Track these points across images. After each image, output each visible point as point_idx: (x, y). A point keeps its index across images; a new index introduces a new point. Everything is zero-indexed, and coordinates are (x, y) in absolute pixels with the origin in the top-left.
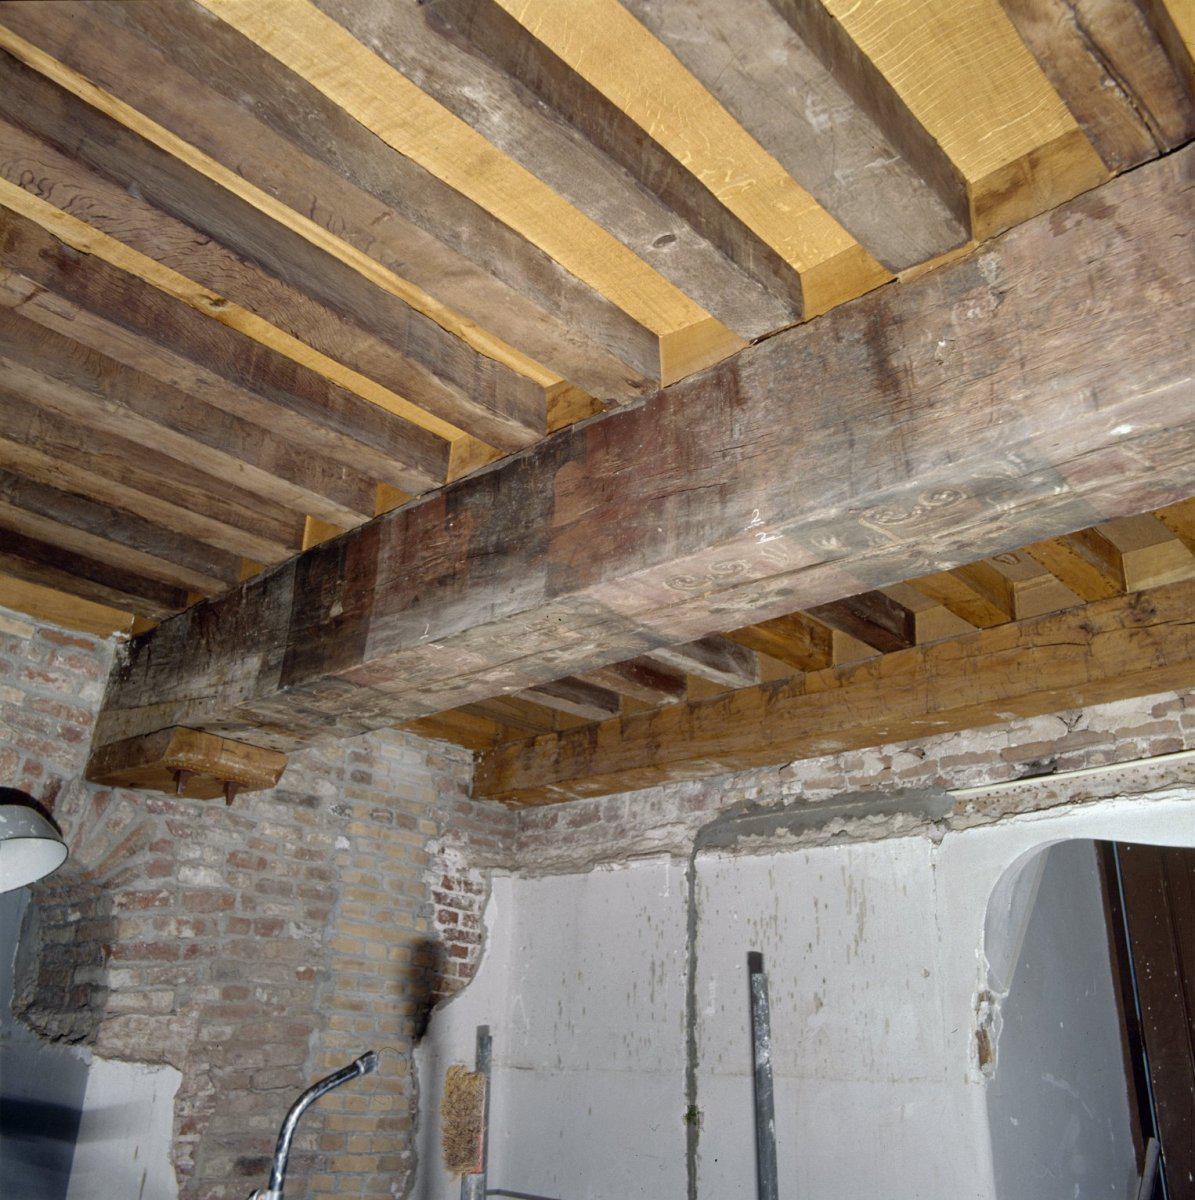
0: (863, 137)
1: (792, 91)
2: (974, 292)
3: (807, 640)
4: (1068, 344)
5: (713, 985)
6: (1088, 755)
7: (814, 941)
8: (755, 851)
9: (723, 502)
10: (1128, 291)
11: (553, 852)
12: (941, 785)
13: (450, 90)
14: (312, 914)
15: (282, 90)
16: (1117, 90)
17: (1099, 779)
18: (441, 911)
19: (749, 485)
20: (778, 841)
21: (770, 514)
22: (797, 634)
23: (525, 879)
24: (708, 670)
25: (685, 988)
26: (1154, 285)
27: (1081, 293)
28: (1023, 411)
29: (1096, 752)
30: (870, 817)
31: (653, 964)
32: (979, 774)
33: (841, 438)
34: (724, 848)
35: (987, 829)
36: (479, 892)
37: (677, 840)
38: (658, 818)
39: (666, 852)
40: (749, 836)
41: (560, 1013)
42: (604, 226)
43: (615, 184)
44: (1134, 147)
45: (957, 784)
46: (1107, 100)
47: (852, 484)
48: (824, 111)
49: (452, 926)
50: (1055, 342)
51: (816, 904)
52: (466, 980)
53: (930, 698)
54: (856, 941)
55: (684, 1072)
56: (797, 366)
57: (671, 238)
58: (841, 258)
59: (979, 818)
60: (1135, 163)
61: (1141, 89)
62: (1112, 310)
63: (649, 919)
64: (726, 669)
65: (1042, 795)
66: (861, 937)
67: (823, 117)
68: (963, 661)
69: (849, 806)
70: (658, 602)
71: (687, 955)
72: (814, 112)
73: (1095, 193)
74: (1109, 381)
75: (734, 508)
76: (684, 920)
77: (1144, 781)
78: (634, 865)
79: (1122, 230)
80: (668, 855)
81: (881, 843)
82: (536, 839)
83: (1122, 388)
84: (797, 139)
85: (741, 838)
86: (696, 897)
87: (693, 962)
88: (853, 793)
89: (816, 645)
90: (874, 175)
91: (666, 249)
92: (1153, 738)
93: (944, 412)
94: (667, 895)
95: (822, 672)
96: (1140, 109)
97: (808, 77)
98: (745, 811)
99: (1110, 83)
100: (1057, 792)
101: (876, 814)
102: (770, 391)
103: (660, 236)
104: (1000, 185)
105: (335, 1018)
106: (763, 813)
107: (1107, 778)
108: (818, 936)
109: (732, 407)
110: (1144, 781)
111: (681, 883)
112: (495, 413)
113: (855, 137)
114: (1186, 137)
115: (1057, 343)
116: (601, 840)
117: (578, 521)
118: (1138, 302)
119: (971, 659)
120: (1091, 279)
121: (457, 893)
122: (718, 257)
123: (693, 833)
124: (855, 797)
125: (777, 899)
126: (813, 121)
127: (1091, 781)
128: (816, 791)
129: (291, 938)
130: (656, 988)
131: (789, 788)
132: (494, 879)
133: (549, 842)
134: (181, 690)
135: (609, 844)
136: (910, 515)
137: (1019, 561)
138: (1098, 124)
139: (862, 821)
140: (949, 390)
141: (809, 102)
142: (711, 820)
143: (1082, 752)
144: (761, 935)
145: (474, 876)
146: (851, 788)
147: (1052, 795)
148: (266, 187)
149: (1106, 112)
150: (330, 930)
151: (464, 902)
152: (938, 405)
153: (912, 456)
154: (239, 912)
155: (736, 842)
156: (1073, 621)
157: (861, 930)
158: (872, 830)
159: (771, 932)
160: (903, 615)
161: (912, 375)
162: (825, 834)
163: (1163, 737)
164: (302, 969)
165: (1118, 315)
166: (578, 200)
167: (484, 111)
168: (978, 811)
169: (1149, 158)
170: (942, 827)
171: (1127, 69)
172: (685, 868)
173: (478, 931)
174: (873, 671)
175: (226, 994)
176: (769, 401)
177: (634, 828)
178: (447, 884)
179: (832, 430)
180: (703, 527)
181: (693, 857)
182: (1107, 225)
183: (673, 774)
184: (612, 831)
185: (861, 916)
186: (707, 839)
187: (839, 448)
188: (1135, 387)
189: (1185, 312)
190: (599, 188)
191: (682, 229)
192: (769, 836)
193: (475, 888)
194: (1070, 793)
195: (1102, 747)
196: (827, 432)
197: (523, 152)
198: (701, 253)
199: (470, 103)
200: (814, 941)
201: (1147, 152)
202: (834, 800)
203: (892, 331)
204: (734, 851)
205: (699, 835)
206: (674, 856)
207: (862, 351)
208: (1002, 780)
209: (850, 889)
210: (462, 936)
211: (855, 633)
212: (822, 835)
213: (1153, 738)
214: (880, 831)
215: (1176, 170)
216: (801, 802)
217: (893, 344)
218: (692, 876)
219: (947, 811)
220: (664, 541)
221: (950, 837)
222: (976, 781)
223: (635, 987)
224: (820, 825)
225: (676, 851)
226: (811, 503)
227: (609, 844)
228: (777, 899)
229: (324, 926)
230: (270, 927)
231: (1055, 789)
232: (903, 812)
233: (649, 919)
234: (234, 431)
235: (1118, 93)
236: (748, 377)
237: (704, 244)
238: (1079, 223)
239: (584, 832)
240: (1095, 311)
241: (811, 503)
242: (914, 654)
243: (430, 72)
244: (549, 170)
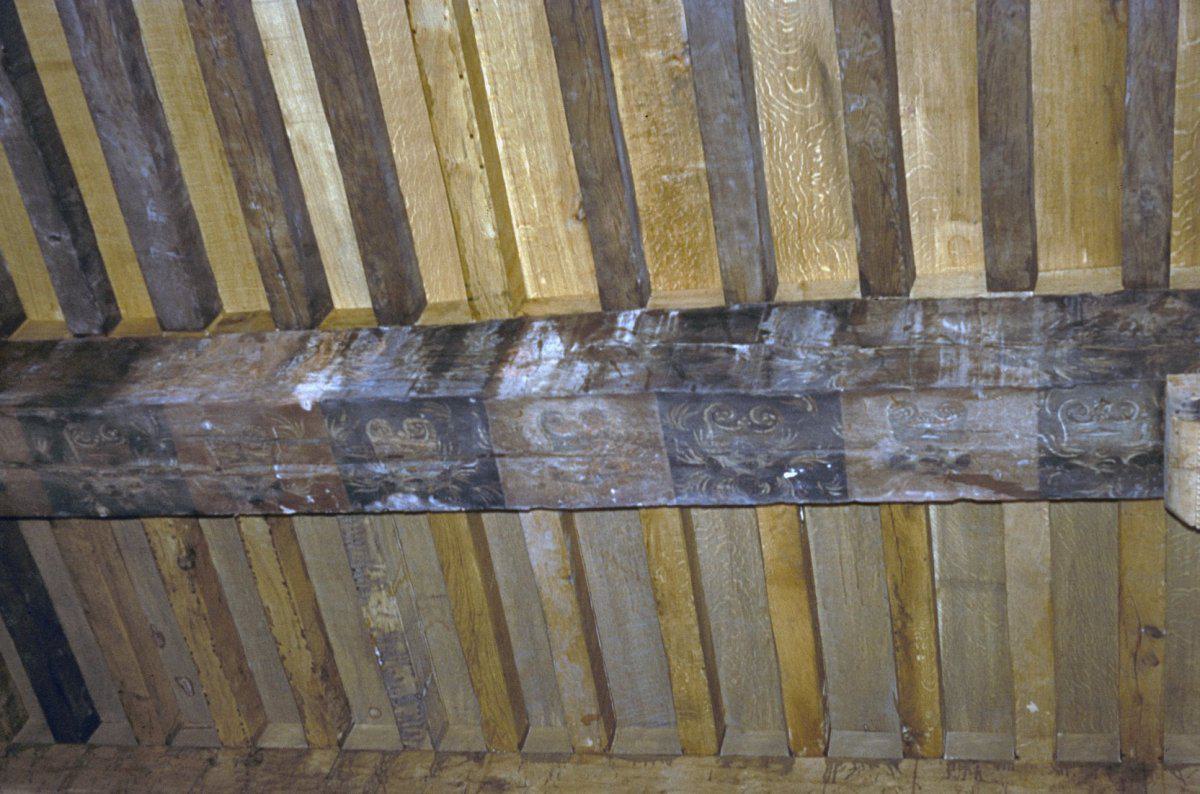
1: (145, 192)
57: (58, 239)
58: (146, 320)
67: (154, 214)
79: (262, 349)
91: (53, 244)
97: (154, 190)
99: (280, 276)
104: (235, 318)
122: (77, 264)
156: (206, 755)
160: (90, 712)
166: (23, 188)
182: (259, 345)
191: (67, 237)
237: (74, 252)
242: (80, 749)
244: (18, 163)
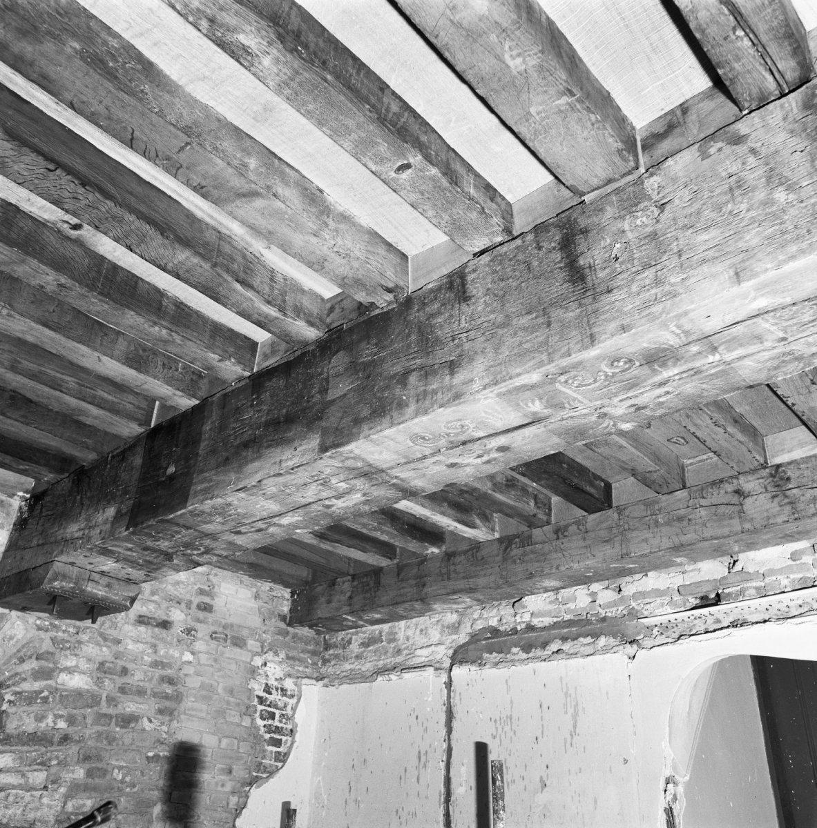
0: (551, 78)
1: (493, 37)
2: (641, 206)
3: (532, 503)
4: (714, 238)
6: (742, 592)
8: (496, 664)
9: (452, 374)
10: (760, 195)
11: (347, 666)
12: (633, 614)
13: (229, 37)
14: (160, 711)
15: (105, 43)
16: (746, 39)
17: (753, 609)
18: (262, 711)
19: (471, 360)
20: (513, 657)
21: (487, 381)
22: (524, 499)
23: (327, 687)
24: (460, 526)
25: (443, 772)
26: (780, 189)
27: (725, 198)
28: (681, 291)
29: (750, 587)
30: (581, 639)
31: (419, 752)
32: (663, 605)
33: (540, 320)
34: (473, 662)
35: (670, 647)
36: (292, 696)
37: (438, 657)
38: (425, 640)
40: (491, 653)
42: (355, 156)
43: (362, 119)
44: (760, 89)
45: (646, 613)
46: (739, 49)
47: (549, 354)
48: (519, 55)
49: (270, 722)
50: (704, 236)
51: (541, 706)
52: (280, 765)
53: (624, 546)
54: (571, 735)
56: (508, 270)
57: (408, 166)
58: (542, 190)
60: (763, 102)
61: (764, 38)
62: (748, 210)
64: (473, 526)
65: (710, 620)
66: (575, 732)
67: (519, 60)
68: (648, 519)
70: (406, 457)
71: (445, 746)
72: (511, 56)
73: (731, 126)
74: (748, 263)
75: (459, 378)
76: (443, 718)
77: (787, 610)
78: (407, 676)
79: (753, 151)
80: (432, 669)
82: (336, 656)
83: (758, 267)
84: (499, 80)
85: (486, 655)
87: (449, 751)
88: (568, 621)
89: (539, 508)
90: (560, 111)
92: (792, 576)
93: (616, 296)
94: (430, 699)
95: (545, 528)
96: (764, 54)
97: (505, 25)
98: (489, 635)
99: (740, 33)
100: (721, 618)
102: (488, 289)
103: (400, 164)
104: (660, 129)
106: (501, 637)
107: (759, 608)
108: (543, 733)
109: (460, 304)
110: (787, 610)
112: (285, 314)
113: (544, 78)
114: (800, 81)
115: (707, 237)
116: (383, 657)
117: (345, 395)
118: (768, 202)
119: (654, 517)
120: (731, 189)
121: (275, 697)
122: (445, 182)
123: (451, 652)
124: (570, 623)
125: (512, 702)
126: (511, 63)
128: (541, 619)
129: (144, 730)
131: (521, 617)
133: (346, 659)
134: (60, 534)
135: (388, 661)
136: (595, 381)
137: (687, 443)
138: (732, 69)
139: (576, 642)
140: (623, 280)
141: (507, 47)
142: (464, 641)
143: (738, 588)
144: (500, 728)
145: (289, 684)
146: (567, 617)
147: (718, 621)
148: (92, 118)
149: (738, 59)
150: (175, 724)
151: (280, 704)
152: (615, 291)
153: (595, 330)
154: (104, 708)
155: (481, 658)
156: (729, 488)
157: (575, 727)
158: (582, 649)
159: (507, 728)
160: (603, 484)
161: (595, 270)
162: (548, 652)
163: (800, 576)
164: (151, 754)
165: (753, 213)
166: (335, 135)
167: (257, 55)
168: (662, 634)
169: (773, 98)
170: (635, 646)
171: (754, 20)
172: (444, 678)
173: (290, 727)
174: (581, 527)
175: (89, 774)
176: (487, 297)
177: (407, 648)
178: (268, 690)
179: (534, 315)
180: (436, 393)
182: (742, 149)
183: (435, 606)
184: (391, 650)
185: (575, 716)
186: (460, 656)
187: (539, 328)
188: (769, 266)
189: (806, 206)
190: (350, 123)
191: (416, 159)
193: (289, 693)
195: (754, 584)
196: (531, 317)
197: (289, 91)
198: (433, 179)
199: (245, 49)
200: (539, 734)
201: (770, 94)
202: (555, 626)
203: (580, 239)
204: (480, 665)
205: (455, 653)
206: (436, 669)
207: (558, 256)
208: (679, 610)
209: (567, 695)
210: (278, 730)
211: (566, 497)
212: (546, 653)
213: (792, 576)
214: (589, 650)
215: (794, 105)
216: (530, 628)
217: (581, 248)
218: (449, 684)
219: (639, 634)
220: (407, 406)
221: (642, 654)
222: (660, 611)
223: (406, 771)
224: (544, 645)
225: (438, 665)
226: (518, 370)
227: (388, 661)
228: (512, 702)
229: (171, 721)
230: (128, 721)
231: (720, 616)
234: (93, 331)
235: (746, 42)
236: (472, 281)
237: (434, 171)
238: (720, 150)
239: (370, 651)
240: (735, 212)
241: (518, 370)
242: (611, 514)
243: (212, 21)
244: (311, 107)
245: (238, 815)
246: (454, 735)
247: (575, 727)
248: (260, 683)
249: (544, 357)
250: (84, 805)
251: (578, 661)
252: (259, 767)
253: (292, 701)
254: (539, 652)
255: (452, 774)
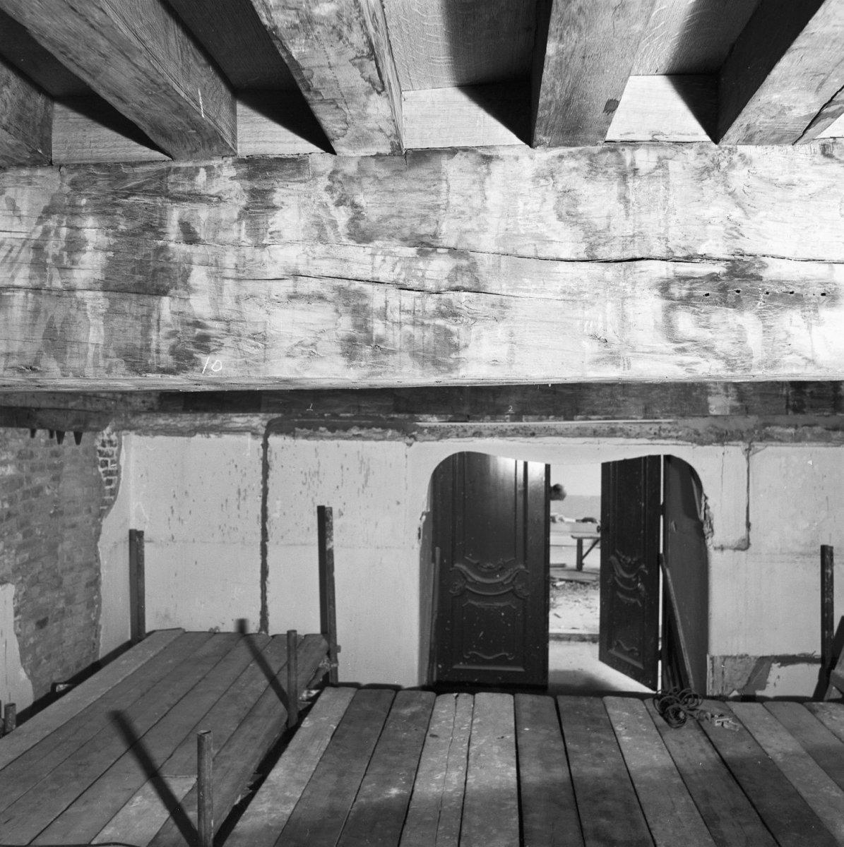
5: (278, 503)
7: (340, 485)
8: (306, 437)
14: (53, 479)
30: (374, 429)
36: (115, 446)
37: (254, 425)
39: (248, 431)
40: (302, 428)
41: (173, 511)
45: (421, 419)
49: (105, 469)
51: (342, 467)
52: (112, 498)
54: (363, 487)
55: (259, 543)
59: (428, 437)
63: (236, 466)
69: (364, 422)
71: (261, 487)
75: (499, 401)
76: (260, 468)
78: (227, 438)
81: (380, 443)
85: (297, 429)
86: (268, 458)
87: (265, 491)
101: (377, 427)
105: (66, 535)
111: (258, 449)
121: (108, 449)
123: (265, 423)
125: (319, 463)
127: (483, 428)
129: (46, 495)
130: (242, 502)
132: (123, 437)
145: (114, 437)
147: (465, 431)
150: (61, 486)
151: (110, 453)
154: (26, 487)
155: (295, 432)
157: (366, 481)
158: (374, 435)
170: (412, 439)
172: (260, 441)
175: (25, 536)
178: (103, 445)
181: (266, 437)
185: (367, 476)
186: (272, 428)
192: (315, 431)
194: (473, 431)
200: (340, 485)
206: (253, 434)
209: (362, 462)
212: (347, 434)
218: (265, 445)
219: (414, 431)
221: (416, 444)
223: (227, 501)
224: (346, 429)
227: (205, 422)
229: (59, 484)
230: (38, 491)
232: (392, 429)
233: (236, 466)
245: (97, 539)
246: (270, 481)
247: (366, 481)
248: (99, 441)
249: (551, 410)
250: (24, 558)
251: (372, 443)
252: (104, 503)
253: (115, 449)
254: (342, 433)
255: (269, 504)
